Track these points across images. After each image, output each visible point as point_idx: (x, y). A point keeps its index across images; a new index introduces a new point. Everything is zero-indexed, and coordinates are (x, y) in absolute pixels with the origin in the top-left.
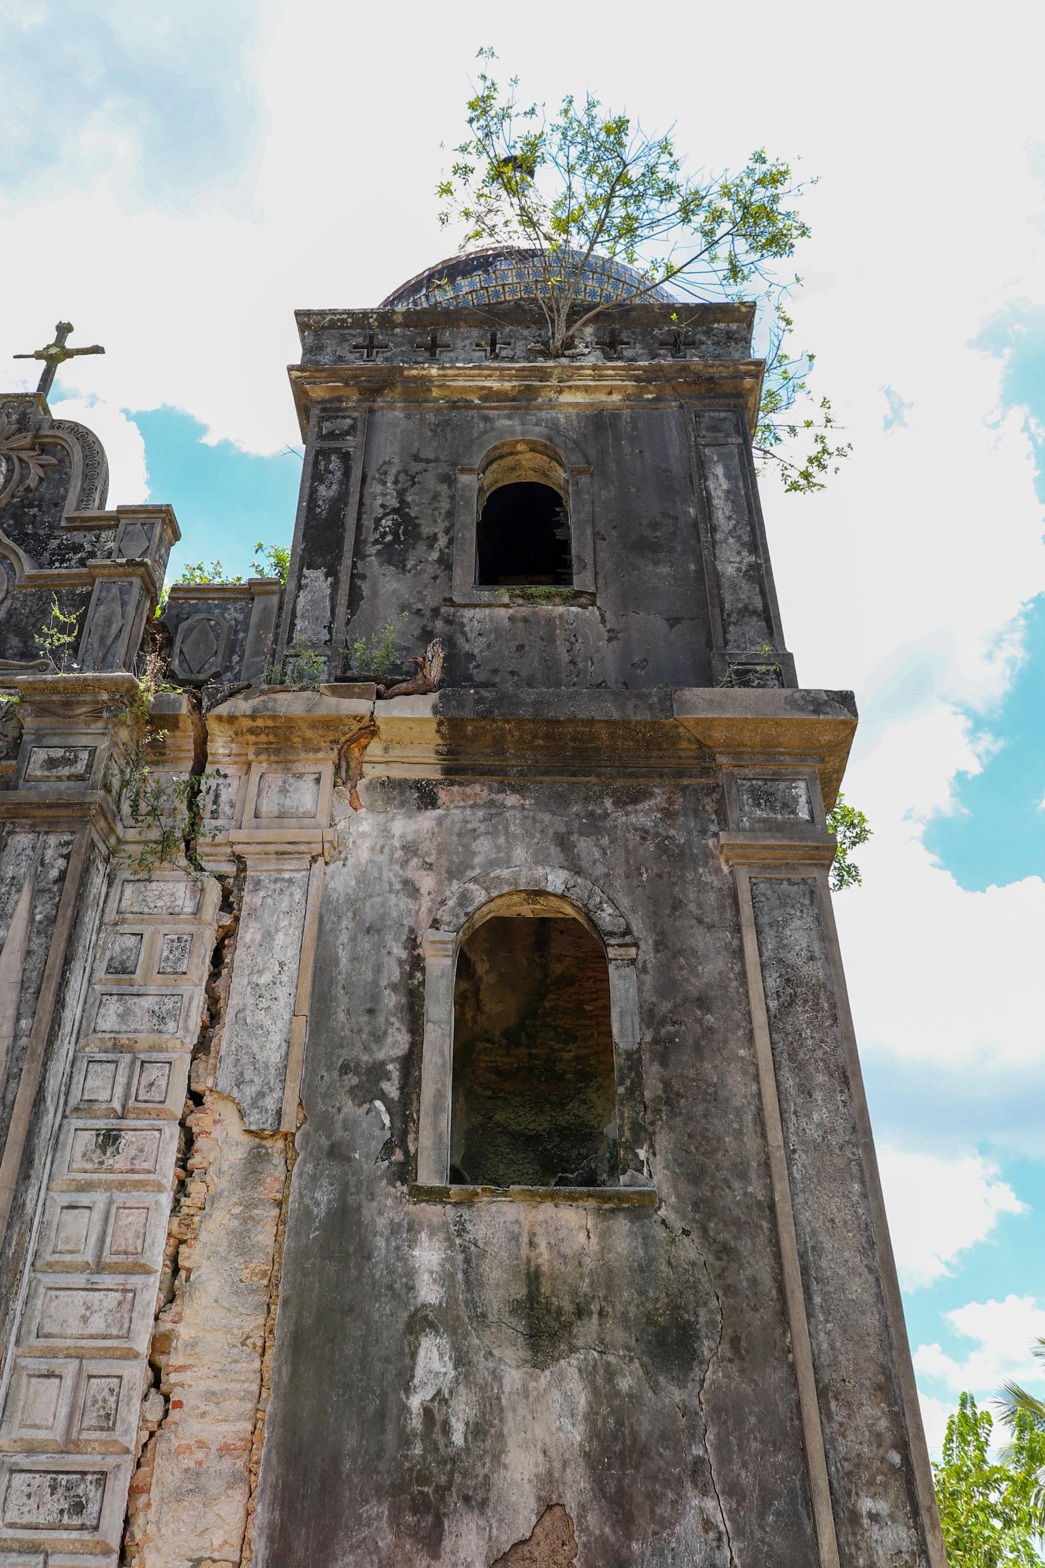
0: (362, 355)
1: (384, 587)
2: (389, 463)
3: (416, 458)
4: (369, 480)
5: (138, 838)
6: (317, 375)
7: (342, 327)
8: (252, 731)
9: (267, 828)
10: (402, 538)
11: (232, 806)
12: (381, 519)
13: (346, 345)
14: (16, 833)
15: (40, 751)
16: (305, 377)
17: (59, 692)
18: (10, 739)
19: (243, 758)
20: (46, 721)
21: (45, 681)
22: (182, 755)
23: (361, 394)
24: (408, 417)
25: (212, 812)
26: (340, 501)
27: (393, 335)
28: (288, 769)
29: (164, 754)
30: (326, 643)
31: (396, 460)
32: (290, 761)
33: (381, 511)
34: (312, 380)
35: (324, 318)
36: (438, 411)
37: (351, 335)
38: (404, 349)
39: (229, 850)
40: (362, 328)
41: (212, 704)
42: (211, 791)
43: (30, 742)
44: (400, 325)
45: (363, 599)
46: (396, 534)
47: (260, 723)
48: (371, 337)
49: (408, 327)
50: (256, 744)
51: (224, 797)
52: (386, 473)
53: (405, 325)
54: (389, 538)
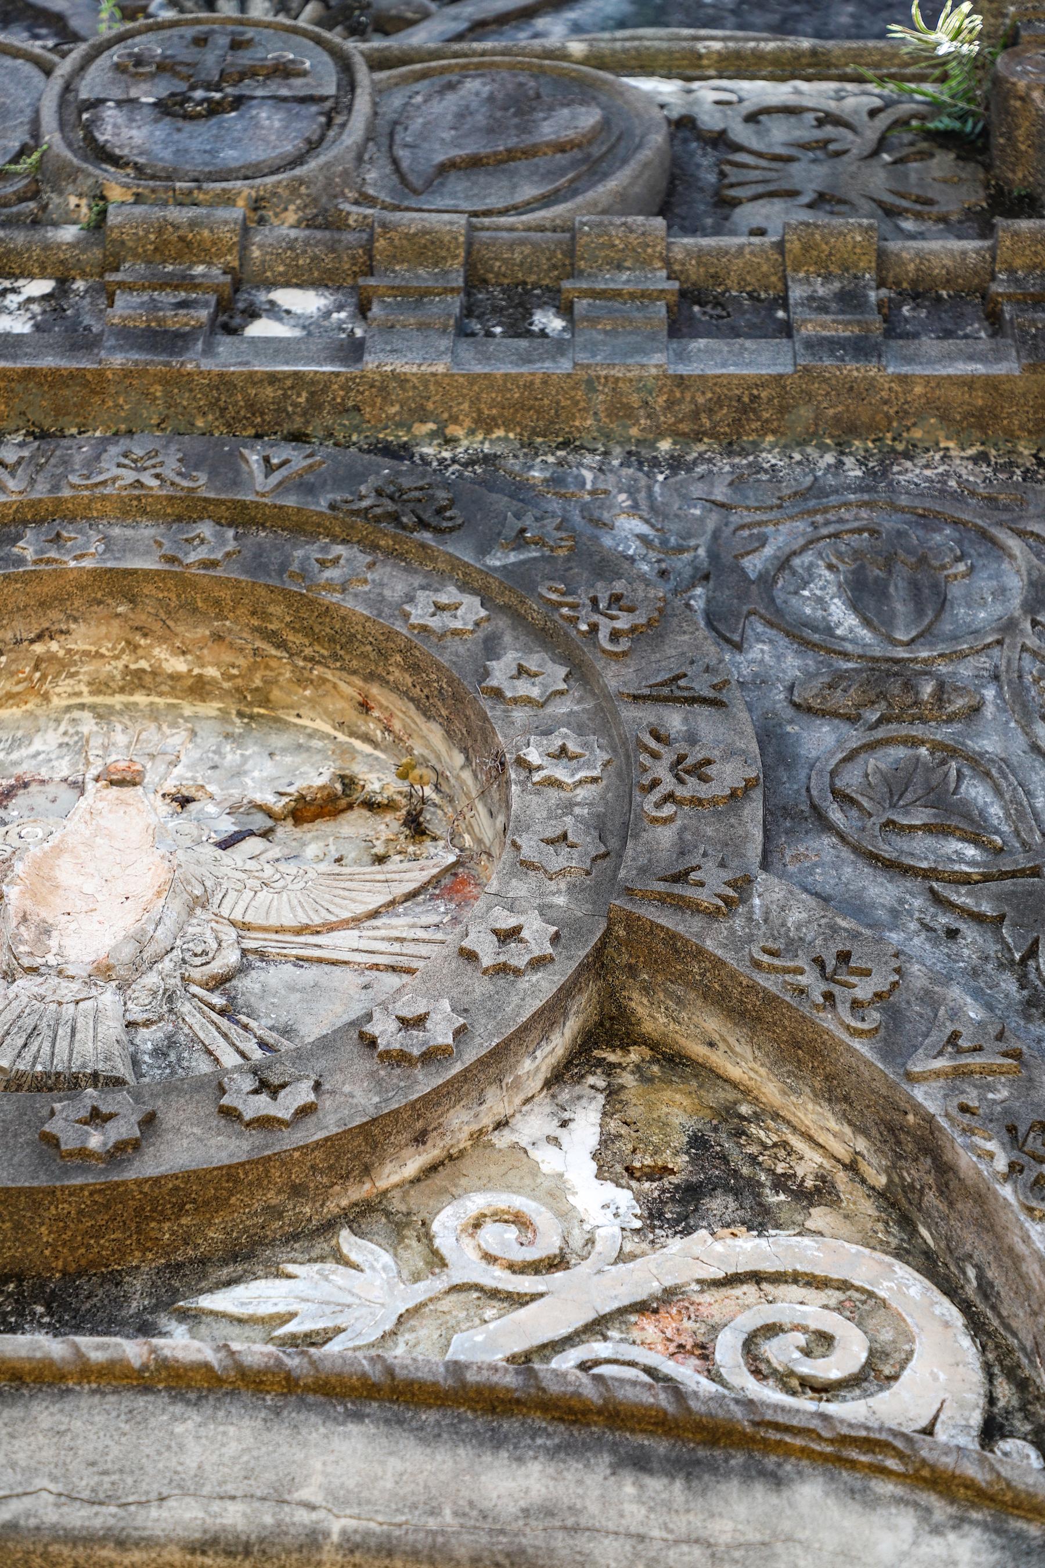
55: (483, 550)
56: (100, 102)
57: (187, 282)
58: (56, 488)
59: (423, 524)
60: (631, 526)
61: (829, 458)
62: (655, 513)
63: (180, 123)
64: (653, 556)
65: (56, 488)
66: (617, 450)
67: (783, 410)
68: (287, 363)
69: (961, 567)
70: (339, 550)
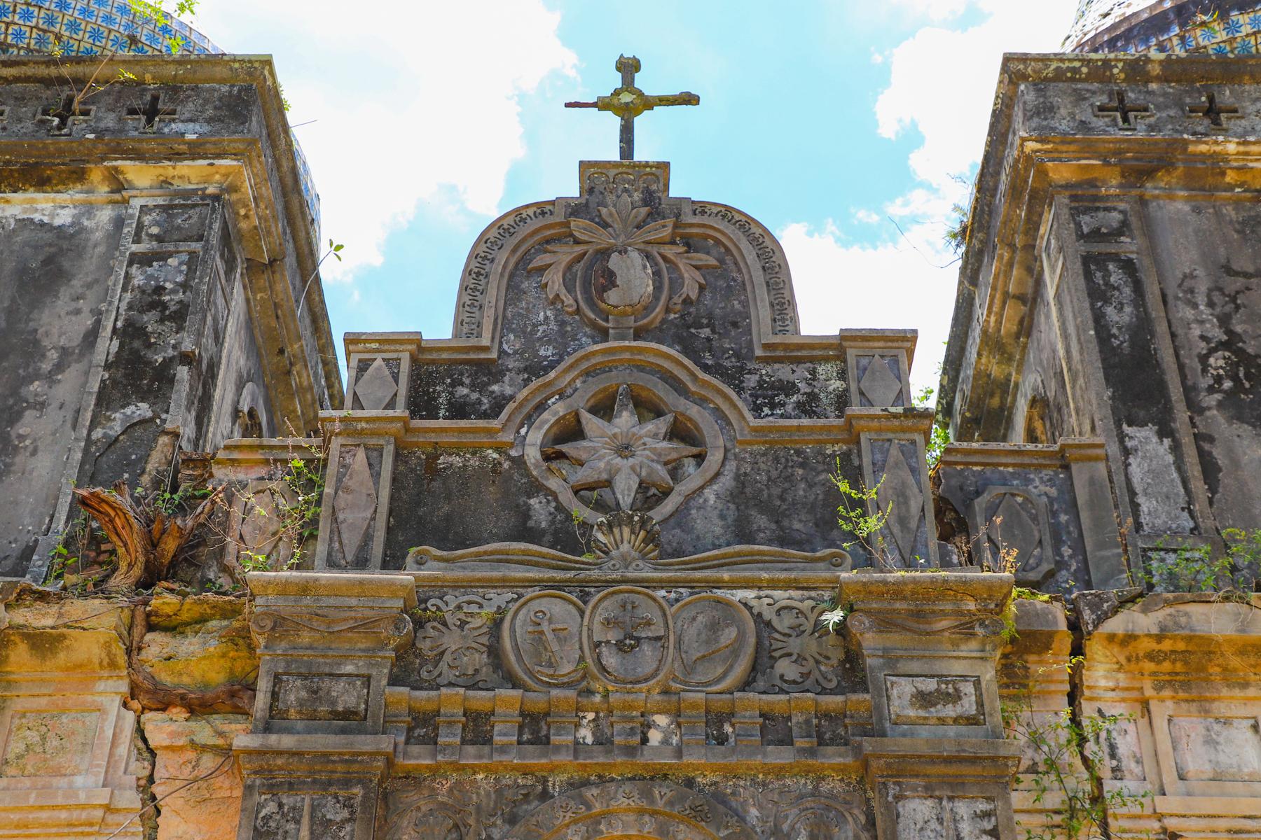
0: (1114, 120)
1: (1245, 454)
2: (1192, 276)
3: (1229, 271)
4: (1170, 299)
5: (1028, 805)
6: (1064, 148)
7: (1072, 80)
8: (1151, 657)
9: (1203, 795)
10: (1247, 385)
11: (1137, 762)
12: (1207, 356)
13: (1085, 105)
14: (906, 797)
15: (903, 681)
16: (1046, 151)
17: (904, 598)
18: (835, 662)
19: (1135, 694)
20: (894, 639)
21: (885, 583)
22: (1053, 687)
23: (1123, 176)
24: (1197, 210)
25: (1114, 770)
26: (1142, 328)
27: (1148, 92)
28: (1207, 712)
29: (1025, 686)
30: (1192, 530)
31: (1200, 272)
32: (1206, 700)
33: (1203, 344)
34: (1056, 155)
35: (1047, 67)
36: (1238, 204)
37: (1088, 90)
38: (1172, 113)
39: (1156, 825)
40: (1101, 82)
41: (1099, 617)
42: (1102, 739)
43: (881, 669)
44: (1158, 79)
45: (1220, 470)
46: (1235, 378)
47: (1167, 645)
48: (1121, 96)
49: (1168, 81)
50: (1153, 674)
51: (1122, 750)
52: (1192, 291)
53: (1164, 79)
54: (1228, 384)
55: (718, 830)
56: (601, 642)
57: (632, 719)
58: (608, 806)
59: (702, 820)
60: (754, 812)
61: (803, 781)
62: (761, 807)
63: (625, 655)
64: (760, 824)
65: (608, 806)
66: (748, 778)
67: (791, 768)
68: (664, 759)
69: (837, 829)
70: (681, 827)
